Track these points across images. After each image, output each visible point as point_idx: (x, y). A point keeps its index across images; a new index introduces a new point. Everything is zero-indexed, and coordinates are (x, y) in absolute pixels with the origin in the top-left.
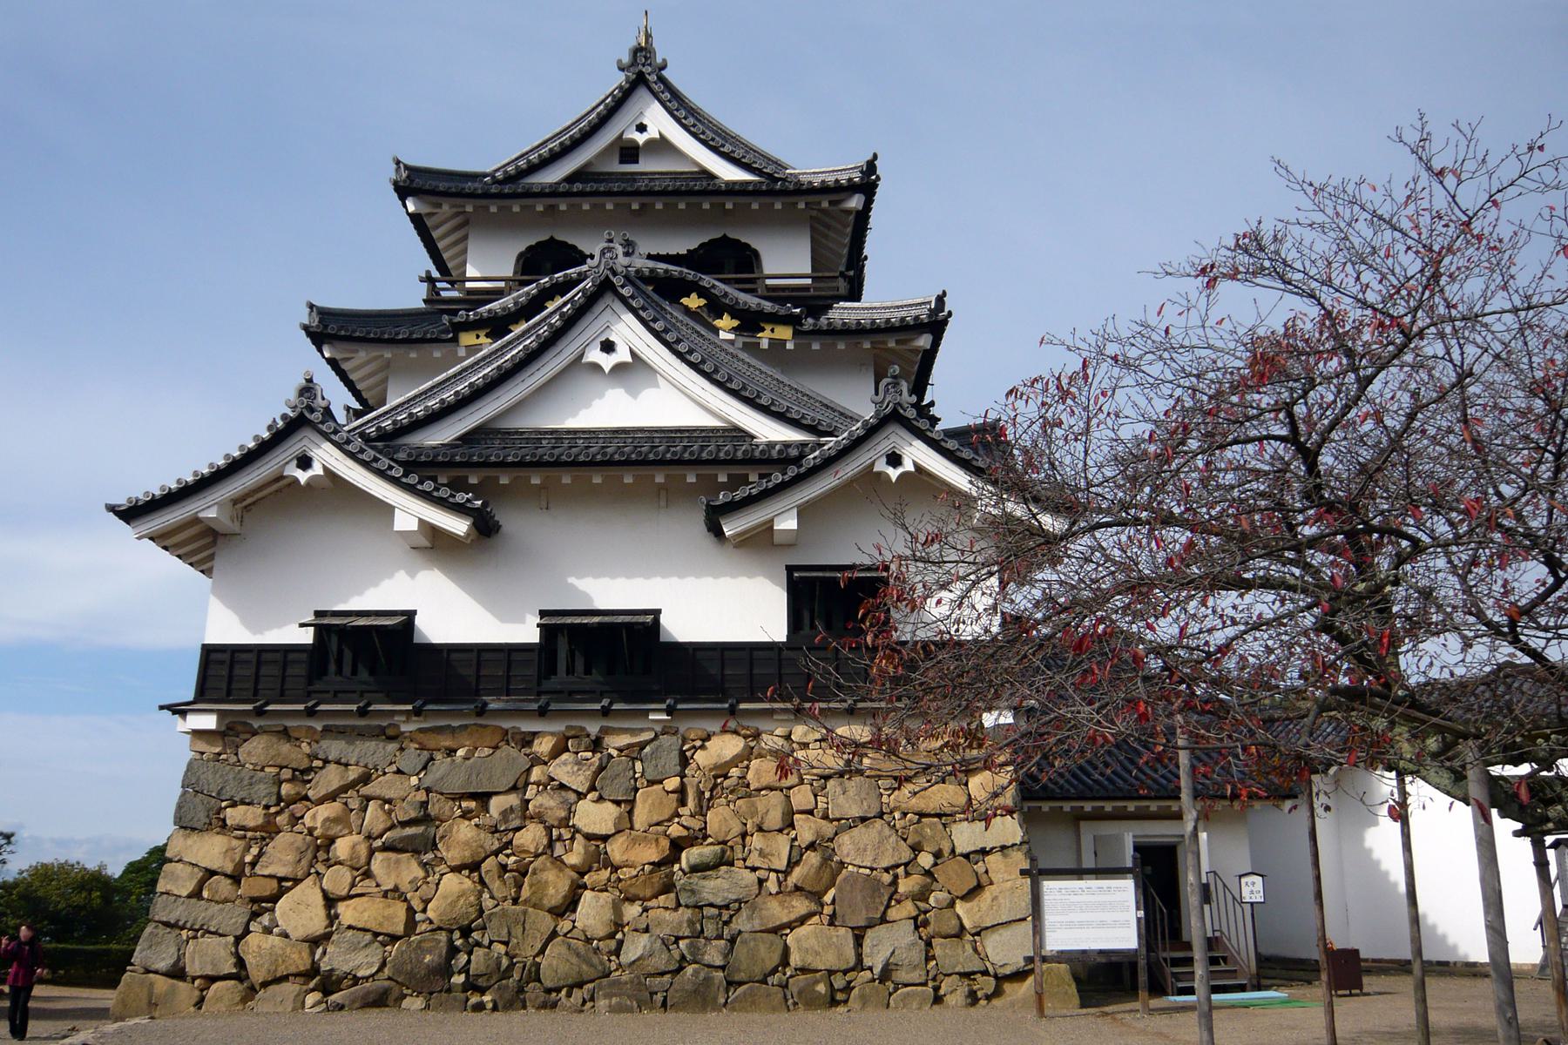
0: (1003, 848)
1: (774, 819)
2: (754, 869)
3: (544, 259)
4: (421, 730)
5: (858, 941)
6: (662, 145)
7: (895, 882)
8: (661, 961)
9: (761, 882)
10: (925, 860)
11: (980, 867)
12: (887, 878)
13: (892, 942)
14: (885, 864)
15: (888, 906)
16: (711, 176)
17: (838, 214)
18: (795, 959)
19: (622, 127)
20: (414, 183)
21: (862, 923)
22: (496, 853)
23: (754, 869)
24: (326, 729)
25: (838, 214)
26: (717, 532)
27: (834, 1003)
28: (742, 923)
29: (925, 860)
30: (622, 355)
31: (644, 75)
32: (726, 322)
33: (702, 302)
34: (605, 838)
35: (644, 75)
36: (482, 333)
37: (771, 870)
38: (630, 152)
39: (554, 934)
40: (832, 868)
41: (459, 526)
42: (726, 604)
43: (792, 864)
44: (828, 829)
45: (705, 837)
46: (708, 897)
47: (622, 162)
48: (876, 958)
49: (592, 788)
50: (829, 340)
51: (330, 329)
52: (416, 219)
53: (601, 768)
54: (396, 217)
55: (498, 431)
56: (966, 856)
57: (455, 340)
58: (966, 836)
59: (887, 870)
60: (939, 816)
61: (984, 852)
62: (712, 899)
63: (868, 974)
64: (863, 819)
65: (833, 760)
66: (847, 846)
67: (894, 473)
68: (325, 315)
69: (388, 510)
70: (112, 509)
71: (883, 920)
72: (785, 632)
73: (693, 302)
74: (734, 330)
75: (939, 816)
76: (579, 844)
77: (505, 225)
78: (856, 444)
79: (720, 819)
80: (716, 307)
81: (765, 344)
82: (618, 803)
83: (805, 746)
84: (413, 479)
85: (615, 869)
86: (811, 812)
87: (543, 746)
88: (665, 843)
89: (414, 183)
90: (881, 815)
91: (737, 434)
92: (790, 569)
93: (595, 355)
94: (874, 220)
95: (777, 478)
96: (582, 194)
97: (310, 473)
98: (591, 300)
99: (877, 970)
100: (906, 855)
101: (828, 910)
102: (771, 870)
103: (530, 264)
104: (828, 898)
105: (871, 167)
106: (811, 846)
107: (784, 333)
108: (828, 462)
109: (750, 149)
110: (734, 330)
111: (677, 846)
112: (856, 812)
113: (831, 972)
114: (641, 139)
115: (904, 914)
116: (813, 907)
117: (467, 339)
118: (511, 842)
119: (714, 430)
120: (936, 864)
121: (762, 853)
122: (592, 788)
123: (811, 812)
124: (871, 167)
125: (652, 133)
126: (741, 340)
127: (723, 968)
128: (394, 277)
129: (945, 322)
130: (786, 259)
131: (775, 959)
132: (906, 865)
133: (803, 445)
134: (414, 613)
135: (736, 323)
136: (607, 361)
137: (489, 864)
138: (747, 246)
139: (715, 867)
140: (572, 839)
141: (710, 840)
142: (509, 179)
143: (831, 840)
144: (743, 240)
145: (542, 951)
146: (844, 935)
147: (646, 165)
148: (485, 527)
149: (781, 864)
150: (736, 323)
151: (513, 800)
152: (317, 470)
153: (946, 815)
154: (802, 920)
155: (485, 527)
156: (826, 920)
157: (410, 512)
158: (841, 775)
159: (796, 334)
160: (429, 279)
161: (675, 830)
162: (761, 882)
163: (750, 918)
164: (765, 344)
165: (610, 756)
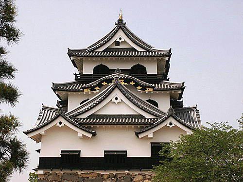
3: (101, 70)
4: (82, 174)
6: (125, 42)
17: (164, 60)
19: (116, 38)
20: (71, 53)
24: (64, 173)
25: (164, 60)
26: (138, 136)
30: (119, 100)
31: (121, 25)
32: (139, 88)
33: (134, 83)
35: (121, 25)
38: (117, 43)
41: (90, 136)
42: (139, 150)
50: (160, 91)
51: (56, 88)
52: (73, 61)
54: (68, 61)
55: (97, 115)
57: (83, 91)
67: (171, 126)
68: (57, 85)
70: (23, 132)
73: (132, 83)
74: (140, 89)
77: (93, 61)
78: (163, 121)
80: (137, 85)
81: (147, 92)
84: (81, 127)
87: (105, 177)
89: (71, 53)
91: (142, 117)
93: (114, 100)
94: (171, 62)
95: (149, 128)
97: (61, 125)
98: (113, 89)
103: (96, 70)
105: (170, 51)
107: (151, 90)
108: (158, 124)
109: (144, 43)
110: (140, 89)
114: (120, 41)
117: (86, 90)
124: (170, 51)
125: (122, 40)
126: (142, 91)
128: (68, 74)
129: (184, 88)
130: (152, 70)
133: (154, 119)
135: (141, 88)
136: (118, 101)
138: (143, 66)
142: (92, 51)
144: (143, 65)
147: (121, 46)
148: (94, 135)
150: (141, 88)
152: (63, 125)
155: (94, 135)
157: (81, 133)
159: (153, 90)
160: (76, 74)
164: (147, 92)
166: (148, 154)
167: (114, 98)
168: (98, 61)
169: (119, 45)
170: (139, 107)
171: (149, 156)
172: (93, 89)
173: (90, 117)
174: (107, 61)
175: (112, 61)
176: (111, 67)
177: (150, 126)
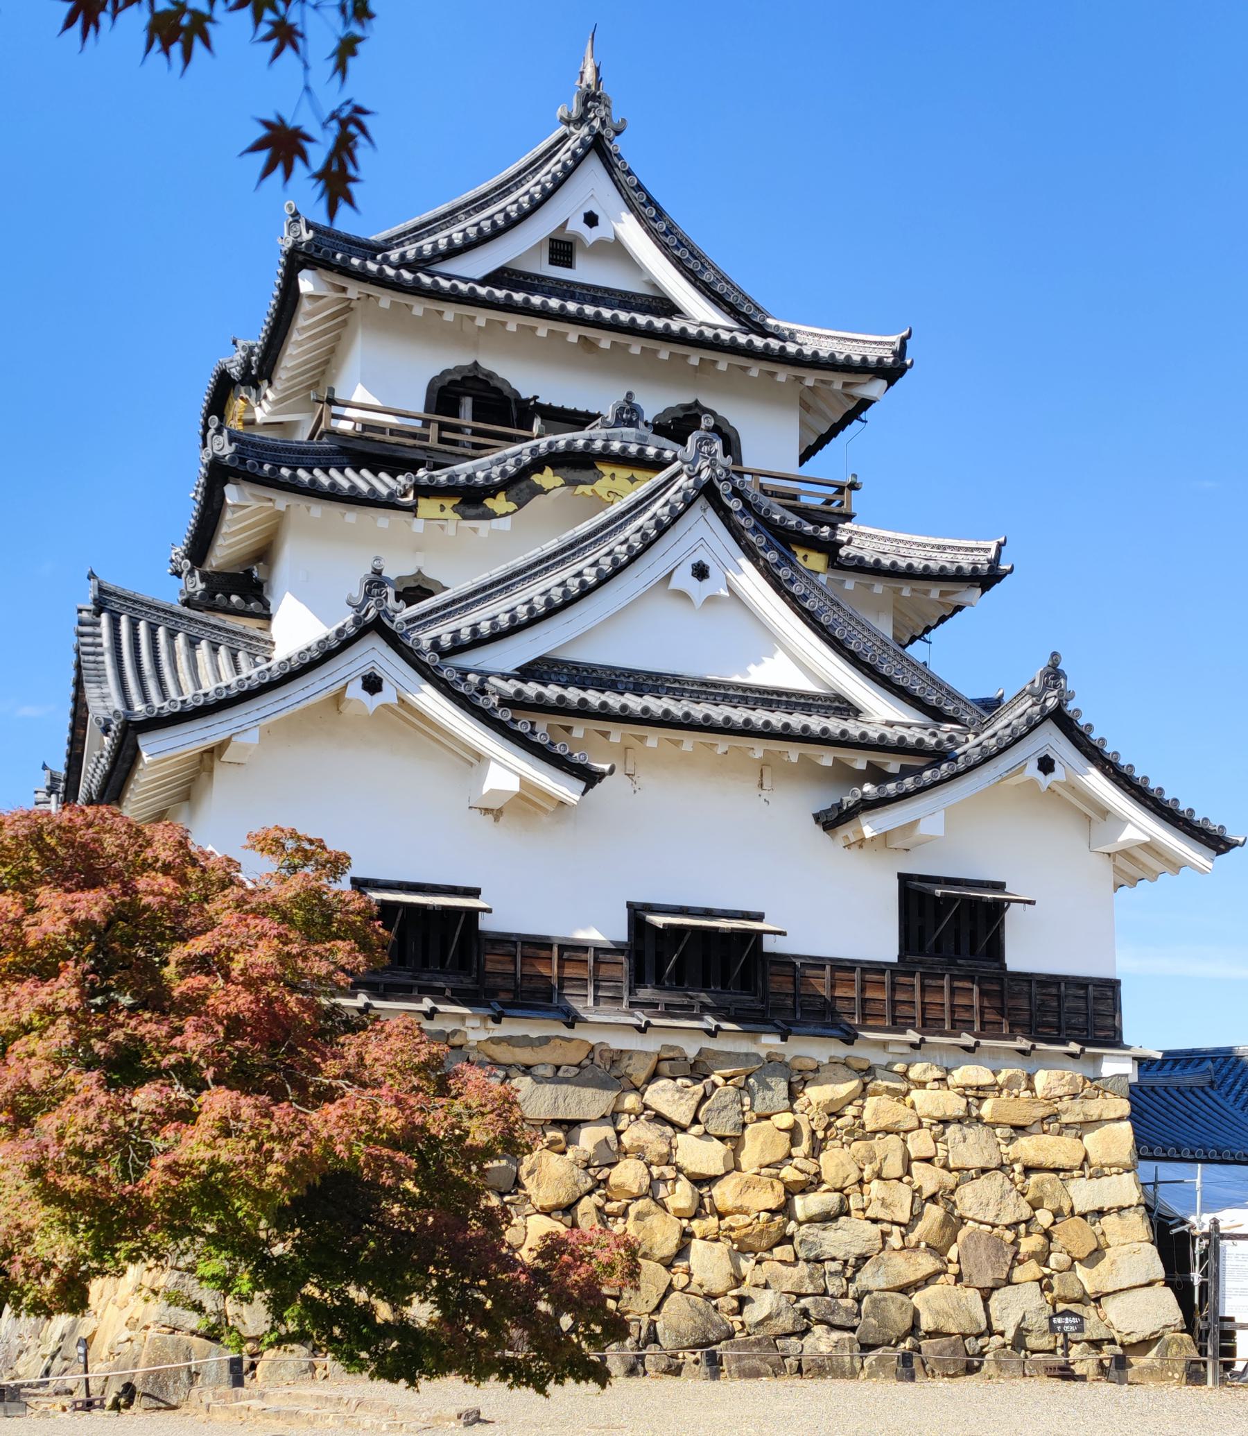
0: (1121, 1209)
1: (894, 1167)
2: (875, 1221)
5: (985, 1300)
7: (1015, 1243)
8: (786, 1322)
9: (885, 1235)
10: (1044, 1217)
11: (1098, 1228)
12: (1009, 1236)
13: (1019, 1305)
14: (1008, 1220)
15: (1012, 1268)
16: (668, 308)
18: (926, 1323)
21: (990, 1284)
22: (590, 1192)
23: (875, 1221)
27: (970, 1370)
28: (868, 1278)
29: (1044, 1218)
34: (710, 1180)
36: (449, 503)
37: (894, 1223)
38: (562, 251)
39: (670, 1288)
40: (952, 1222)
41: (565, 788)
42: (835, 909)
43: (916, 1217)
44: (950, 1179)
45: (821, 1182)
46: (828, 1250)
47: (553, 262)
48: (1007, 1324)
49: (696, 1121)
53: (705, 1098)
55: (565, 663)
56: (1084, 1216)
57: (412, 509)
58: (1083, 1194)
59: (1008, 1227)
60: (1056, 1170)
61: (1100, 1213)
62: (834, 1254)
63: (996, 1340)
64: (984, 1171)
65: (954, 1105)
66: (969, 1199)
69: (480, 758)
71: (1009, 1282)
72: (897, 952)
75: (1056, 1170)
76: (684, 1186)
79: (836, 1163)
82: (722, 1139)
83: (922, 1085)
85: (721, 1216)
86: (929, 1160)
88: (779, 1188)
90: (1001, 1167)
91: (845, 707)
92: (904, 879)
96: (508, 307)
99: (1010, 1334)
100: (1026, 1212)
101: (953, 1269)
102: (894, 1223)
103: (444, 396)
104: (953, 1253)
106: (933, 1198)
111: (792, 1190)
112: (977, 1162)
113: (965, 1336)
115: (1030, 1276)
116: (939, 1265)
117: (428, 507)
118: (605, 1181)
119: (815, 697)
120: (1054, 1223)
121: (884, 1203)
122: (696, 1121)
123: (929, 1160)
127: (853, 1329)
131: (908, 1323)
132: (1026, 1222)
134: (630, 905)
137: (587, 1204)
139: (835, 1218)
140: (675, 1180)
141: (825, 1187)
143: (952, 1192)
145: (658, 1309)
146: (974, 1297)
147: (584, 272)
149: (904, 1217)
151: (607, 1131)
153: (1064, 1170)
154: (928, 1280)
156: (952, 1279)
157: (507, 769)
158: (959, 1121)
161: (789, 1173)
162: (885, 1235)
163: (874, 1275)
165: (715, 1086)
166: (880, 941)
167: (686, 569)
168: (458, 336)
169: (569, 264)
170: (838, 646)
171: (896, 960)
172: (471, 499)
173: (527, 673)
174: (525, 347)
175: (552, 353)
176: (528, 380)
177: (921, 767)
